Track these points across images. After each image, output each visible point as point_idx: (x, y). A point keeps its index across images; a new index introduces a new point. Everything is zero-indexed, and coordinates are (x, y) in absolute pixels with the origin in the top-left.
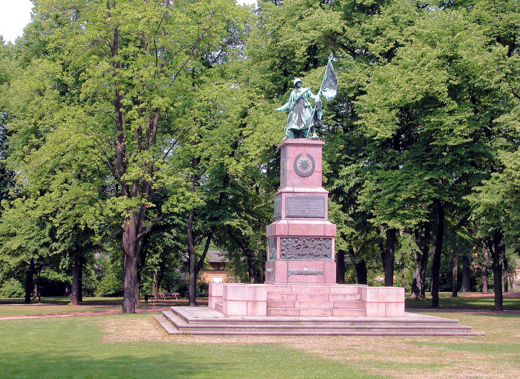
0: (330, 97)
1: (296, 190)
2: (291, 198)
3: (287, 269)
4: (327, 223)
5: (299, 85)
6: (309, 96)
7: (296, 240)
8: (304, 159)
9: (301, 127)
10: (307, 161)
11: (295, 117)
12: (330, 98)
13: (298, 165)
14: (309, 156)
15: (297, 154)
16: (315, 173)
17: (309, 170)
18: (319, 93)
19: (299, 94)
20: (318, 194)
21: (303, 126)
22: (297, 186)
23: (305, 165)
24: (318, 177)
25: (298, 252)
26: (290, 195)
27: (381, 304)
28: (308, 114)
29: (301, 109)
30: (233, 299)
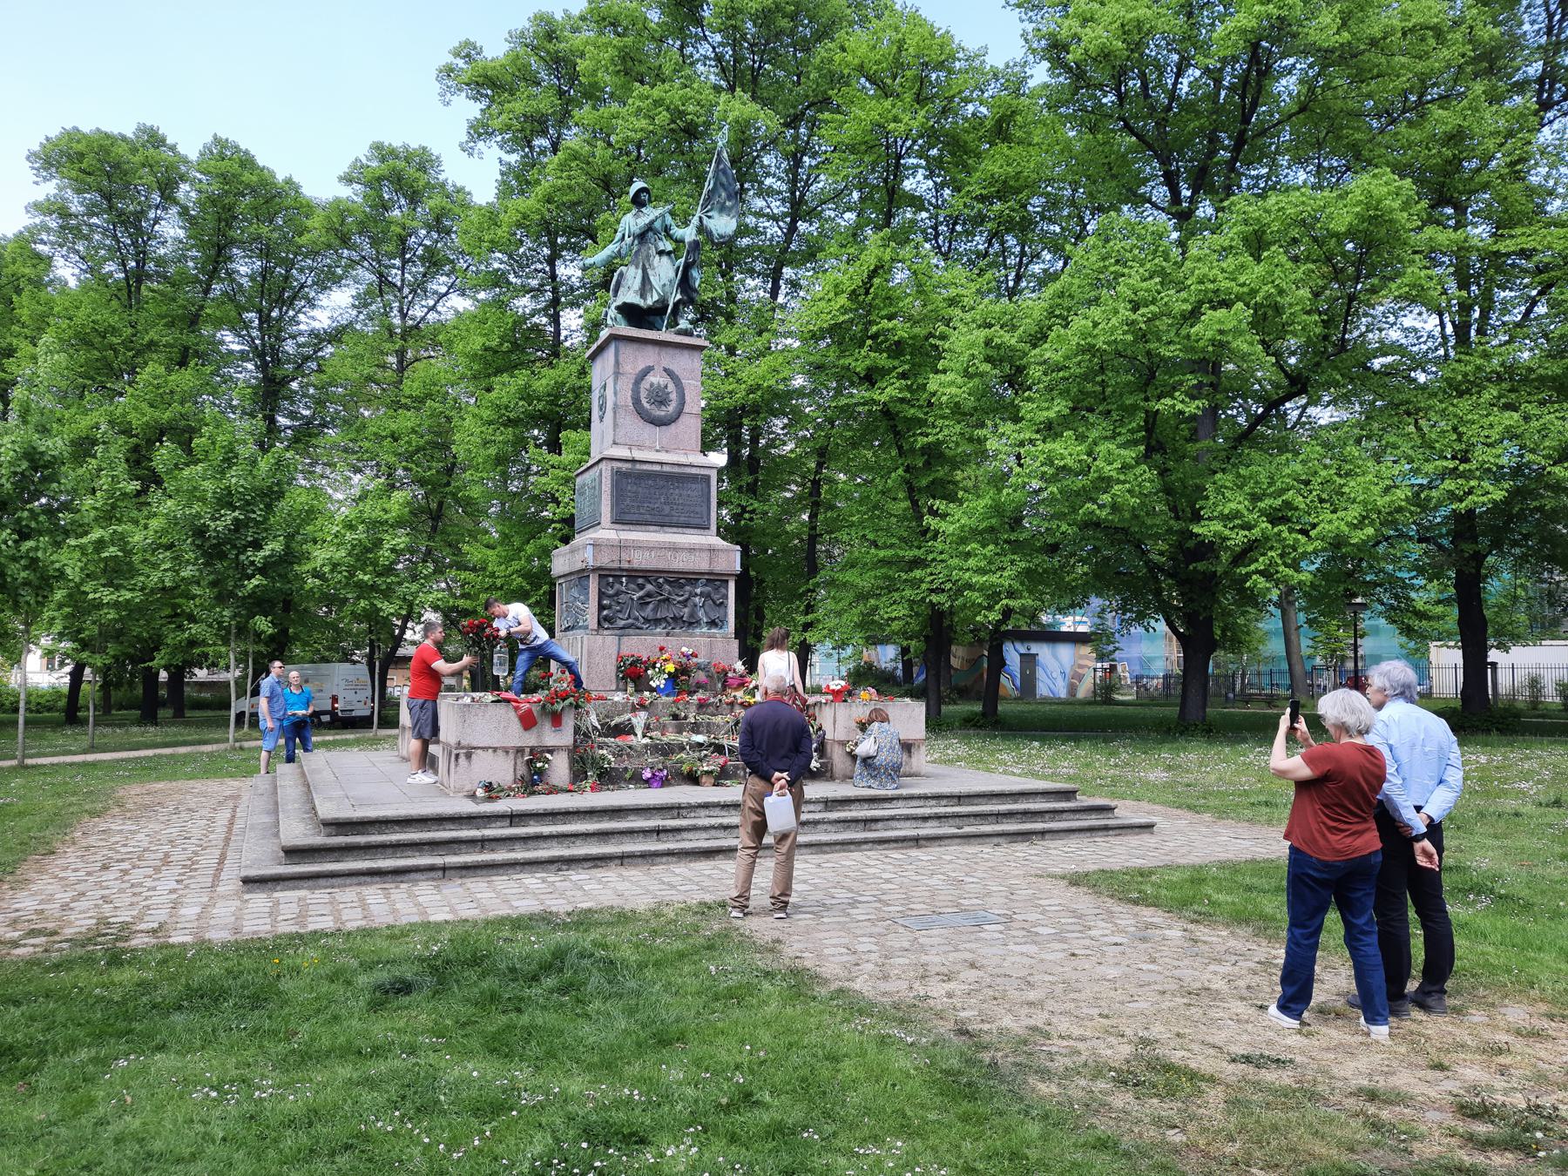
0: (722, 231)
1: (638, 455)
5: (644, 196)
6: (667, 229)
7: (640, 581)
8: (656, 379)
9: (650, 302)
12: (721, 237)
15: (641, 366)
16: (683, 419)
18: (695, 221)
19: (644, 221)
21: (656, 297)
23: (660, 398)
24: (690, 427)
25: (648, 611)
28: (664, 272)
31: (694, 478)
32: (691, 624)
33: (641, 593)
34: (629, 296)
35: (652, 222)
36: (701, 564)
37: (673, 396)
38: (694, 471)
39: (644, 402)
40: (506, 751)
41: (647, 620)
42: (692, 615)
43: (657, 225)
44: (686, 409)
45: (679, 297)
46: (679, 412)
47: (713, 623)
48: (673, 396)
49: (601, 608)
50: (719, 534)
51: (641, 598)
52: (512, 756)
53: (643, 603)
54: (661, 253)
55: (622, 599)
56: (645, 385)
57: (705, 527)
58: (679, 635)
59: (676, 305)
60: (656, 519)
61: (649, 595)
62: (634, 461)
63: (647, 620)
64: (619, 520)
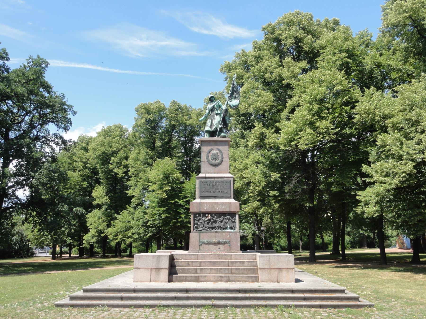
2: (203, 182)
3: (199, 239)
4: (233, 201)
8: (213, 152)
10: (217, 154)
11: (209, 122)
13: (210, 157)
14: (218, 150)
16: (223, 163)
17: (219, 161)
20: (225, 179)
22: (210, 173)
26: (203, 180)
27: (272, 271)
28: (217, 119)
29: (213, 116)
30: (139, 267)
31: (225, 182)
32: (224, 229)
33: (207, 219)
34: (207, 128)
35: (214, 106)
36: (226, 209)
37: (220, 156)
38: (225, 179)
39: (210, 159)
40: (148, 269)
41: (209, 228)
42: (224, 226)
43: (215, 106)
44: (224, 160)
45: (221, 126)
46: (222, 161)
47: (231, 228)
48: (220, 156)
49: (194, 224)
50: (234, 198)
51: (206, 221)
52: (150, 270)
53: (208, 222)
54: (217, 114)
55: (201, 221)
56: (211, 154)
57: (229, 197)
58: (220, 232)
59: (221, 129)
60: (214, 195)
61: (210, 220)
62: (206, 178)
63: (209, 228)
64: (201, 197)
